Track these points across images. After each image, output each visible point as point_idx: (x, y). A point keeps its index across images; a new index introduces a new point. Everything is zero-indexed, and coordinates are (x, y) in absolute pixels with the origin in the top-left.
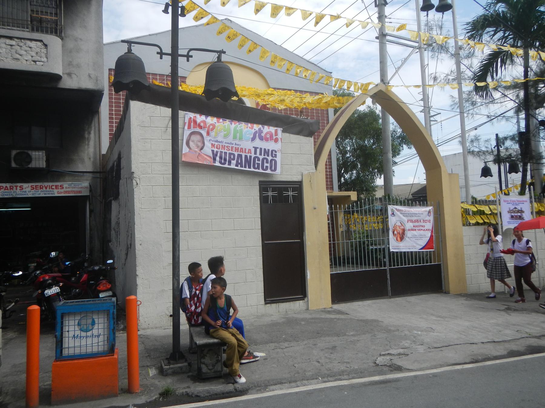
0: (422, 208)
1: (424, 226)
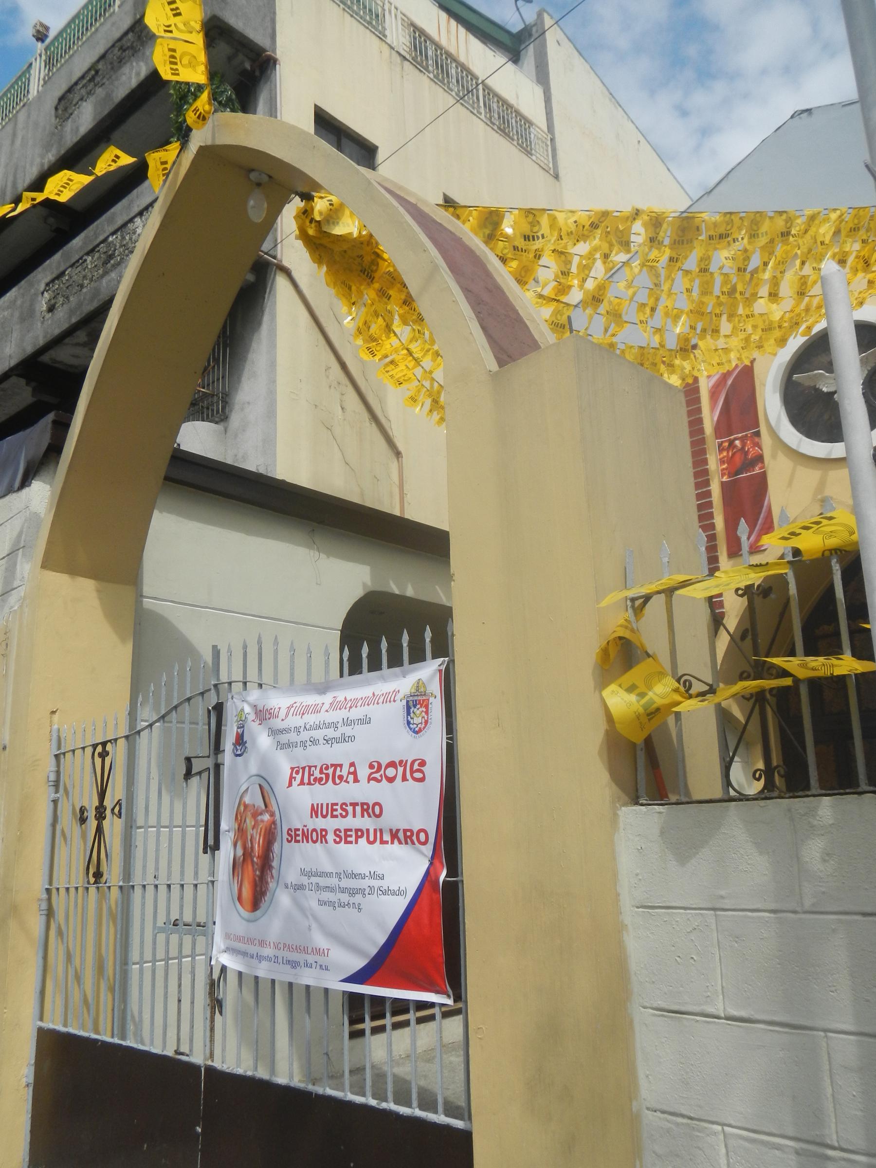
0: (384, 679)
1: (370, 809)
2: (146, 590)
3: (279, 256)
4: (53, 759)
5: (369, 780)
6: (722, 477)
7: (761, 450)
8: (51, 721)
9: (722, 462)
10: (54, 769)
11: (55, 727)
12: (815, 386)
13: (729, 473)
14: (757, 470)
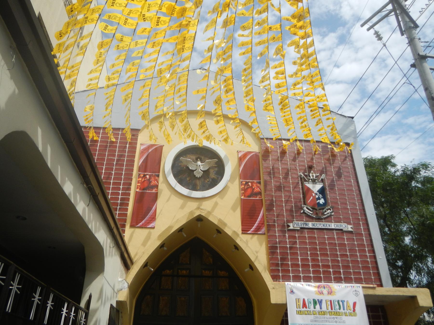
6: (137, 189)
7: (158, 183)
9: (138, 182)
12: (187, 165)
13: (140, 188)
14: (154, 191)
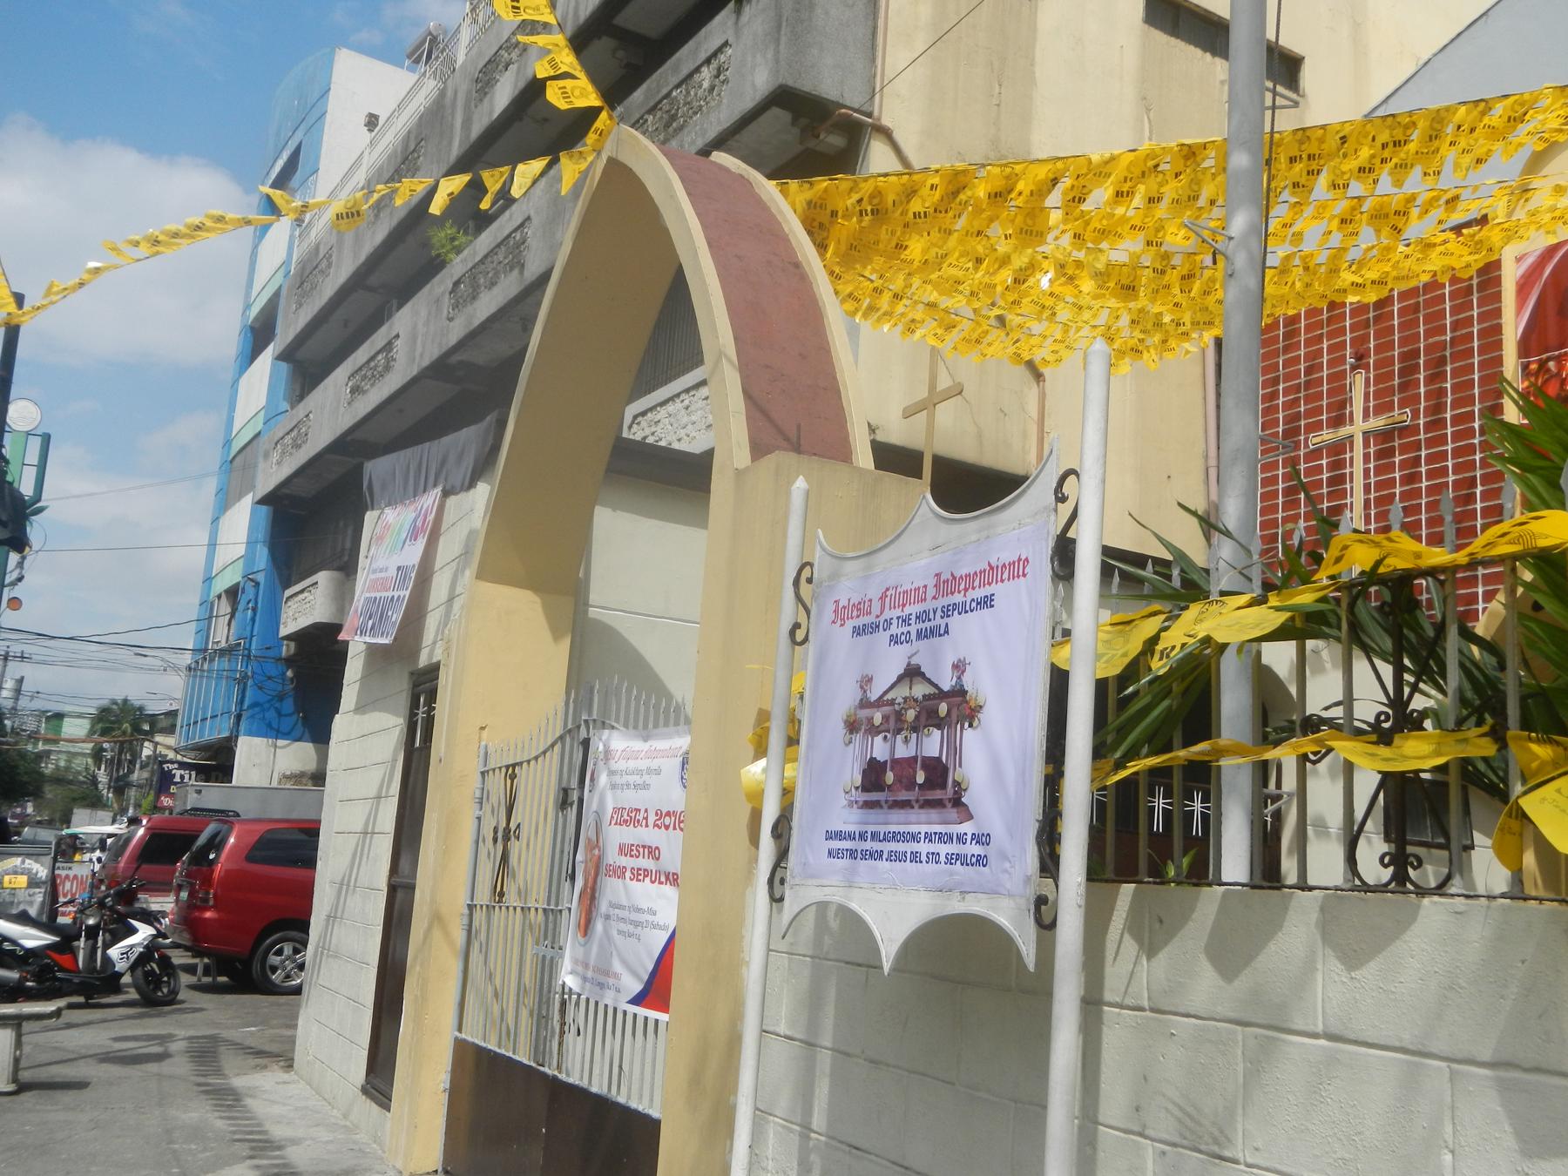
1: (653, 852)
2: (593, 597)
3: (876, 113)
4: (479, 775)
5: (655, 825)
8: (480, 738)
10: (480, 786)
11: (483, 743)
